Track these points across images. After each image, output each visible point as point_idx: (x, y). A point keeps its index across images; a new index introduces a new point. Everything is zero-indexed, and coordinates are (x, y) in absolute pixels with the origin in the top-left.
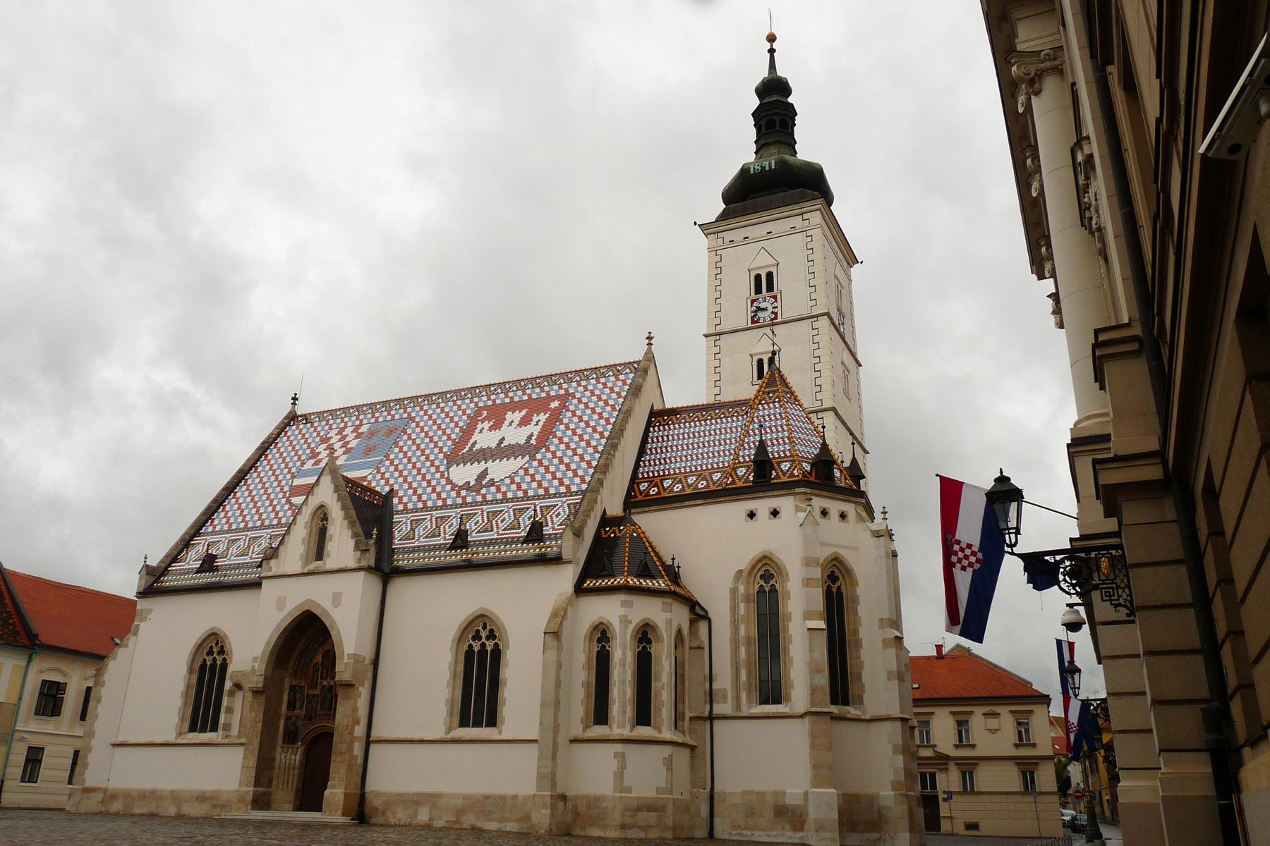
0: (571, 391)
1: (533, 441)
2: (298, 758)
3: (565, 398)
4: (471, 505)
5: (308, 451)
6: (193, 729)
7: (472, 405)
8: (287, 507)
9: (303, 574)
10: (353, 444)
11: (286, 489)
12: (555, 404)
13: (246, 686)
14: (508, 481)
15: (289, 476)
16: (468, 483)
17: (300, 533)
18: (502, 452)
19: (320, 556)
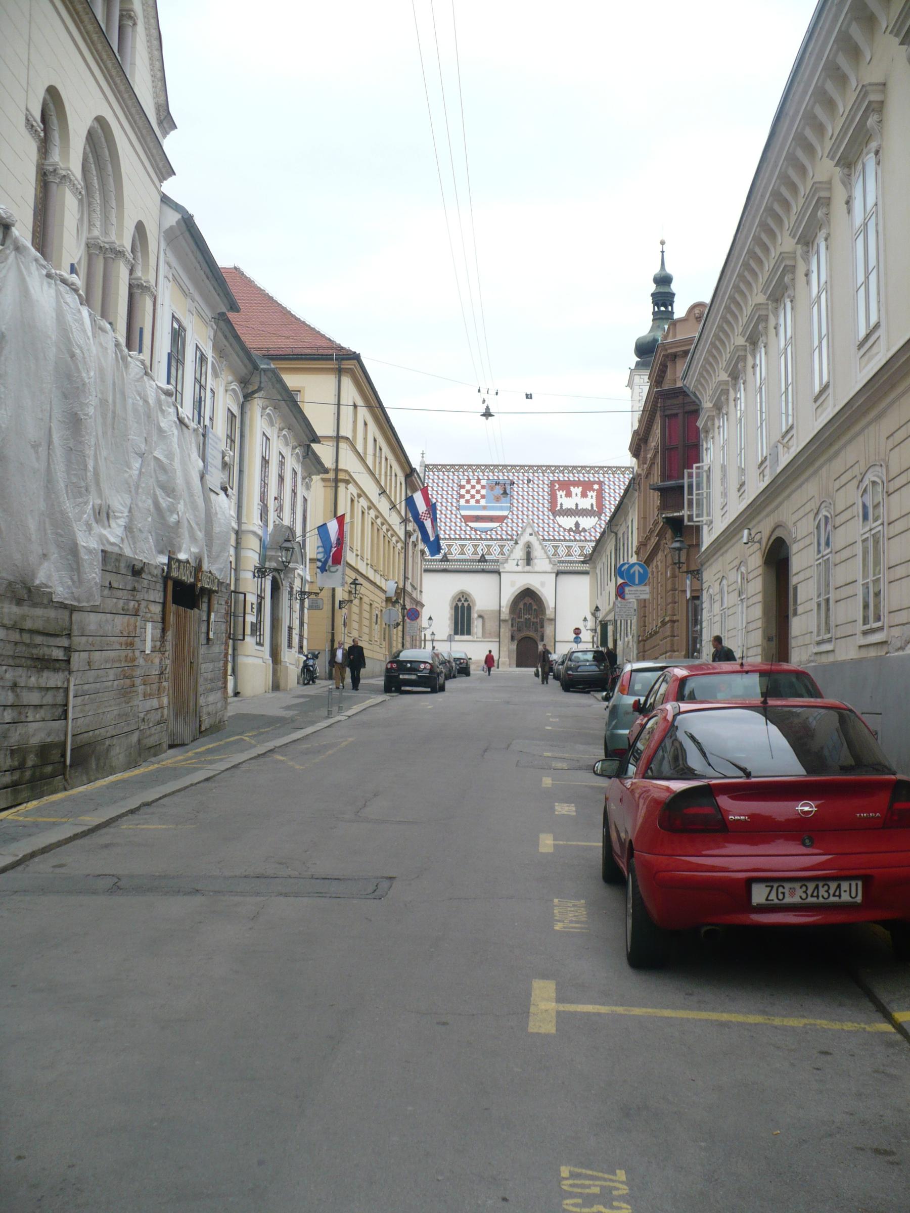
0: (602, 479)
1: (595, 508)
2: (515, 647)
3: (600, 483)
4: (581, 541)
5: (455, 492)
6: (456, 633)
7: (546, 478)
8: (468, 528)
9: (524, 572)
10: (483, 492)
11: (459, 516)
12: (596, 487)
13: (486, 617)
14: (592, 530)
15: (454, 508)
16: (571, 528)
17: (519, 553)
18: (576, 512)
19: (528, 564)
